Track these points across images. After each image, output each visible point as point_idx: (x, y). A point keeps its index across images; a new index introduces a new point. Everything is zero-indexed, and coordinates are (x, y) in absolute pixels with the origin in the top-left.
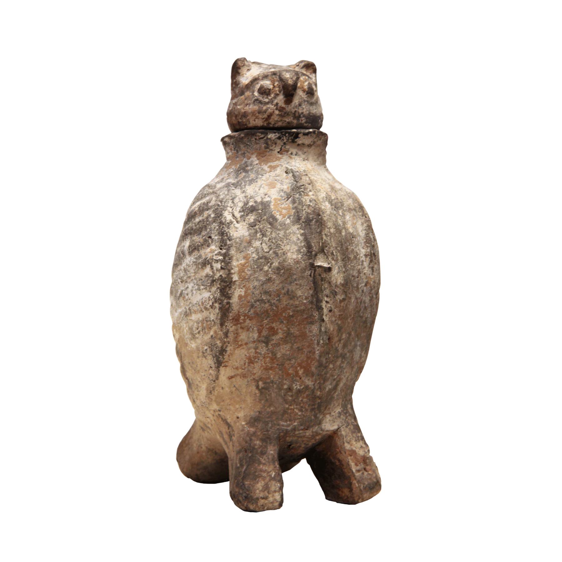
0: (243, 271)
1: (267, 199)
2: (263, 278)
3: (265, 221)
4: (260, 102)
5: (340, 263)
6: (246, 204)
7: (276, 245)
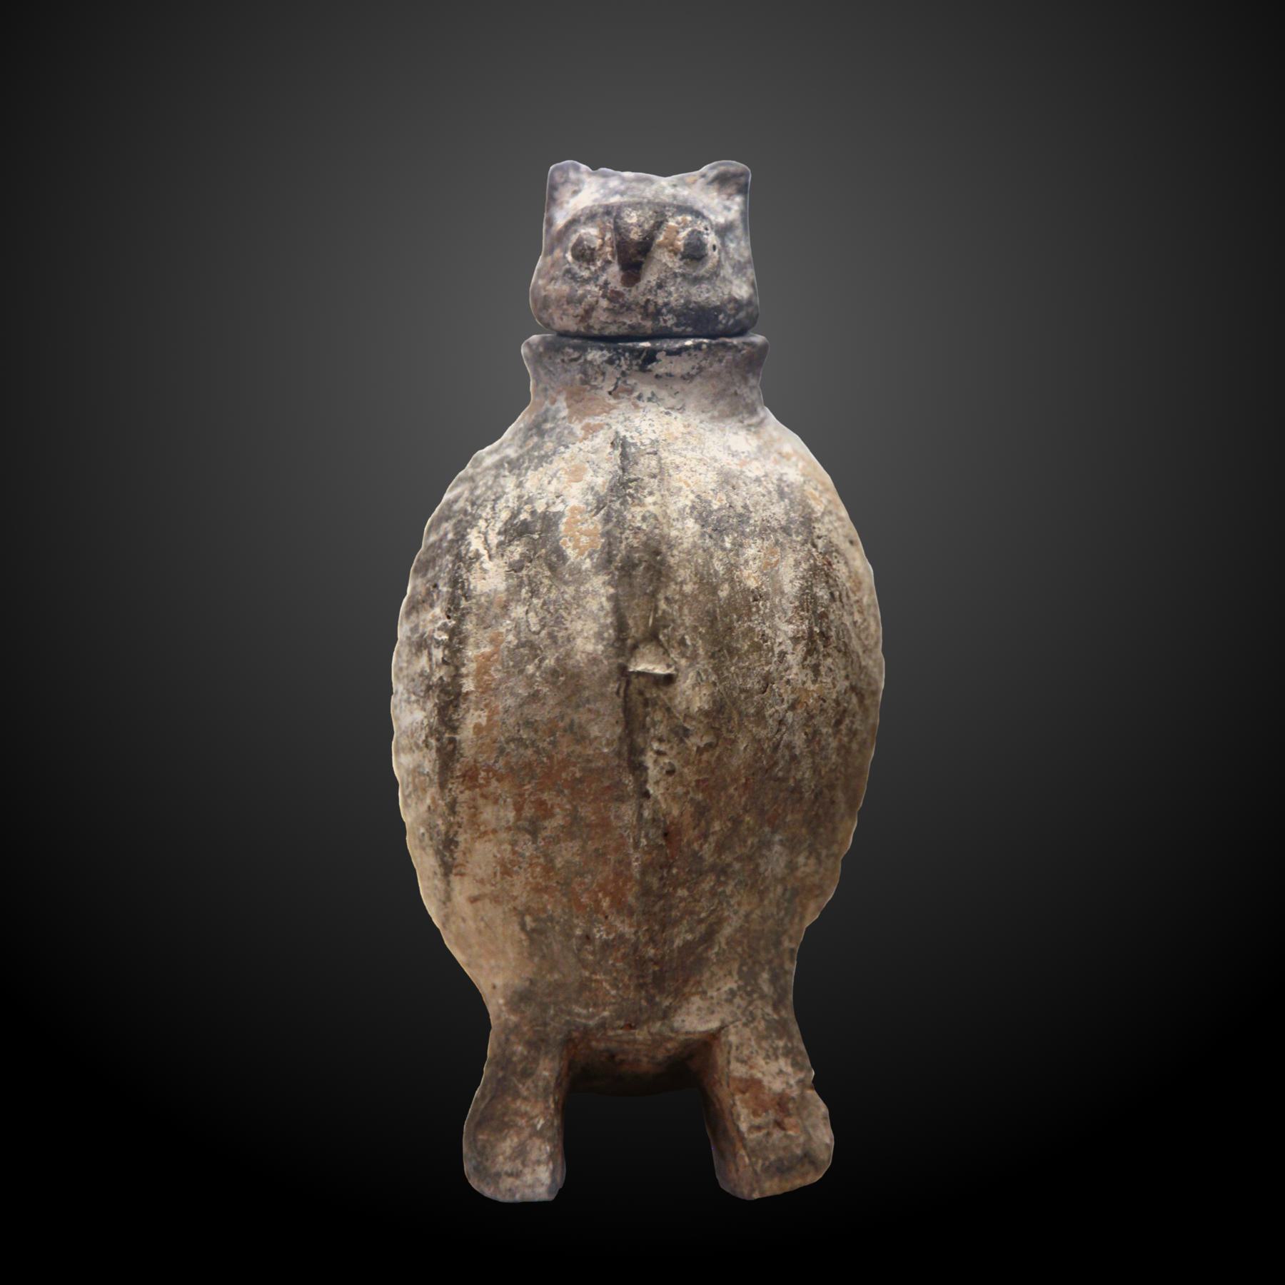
0: (486, 672)
1: (559, 507)
2: (523, 692)
3: (541, 561)
4: (574, 277)
5: (703, 663)
6: (514, 515)
7: (554, 618)
